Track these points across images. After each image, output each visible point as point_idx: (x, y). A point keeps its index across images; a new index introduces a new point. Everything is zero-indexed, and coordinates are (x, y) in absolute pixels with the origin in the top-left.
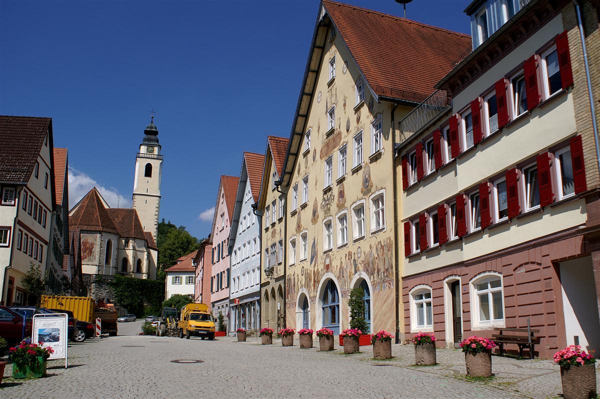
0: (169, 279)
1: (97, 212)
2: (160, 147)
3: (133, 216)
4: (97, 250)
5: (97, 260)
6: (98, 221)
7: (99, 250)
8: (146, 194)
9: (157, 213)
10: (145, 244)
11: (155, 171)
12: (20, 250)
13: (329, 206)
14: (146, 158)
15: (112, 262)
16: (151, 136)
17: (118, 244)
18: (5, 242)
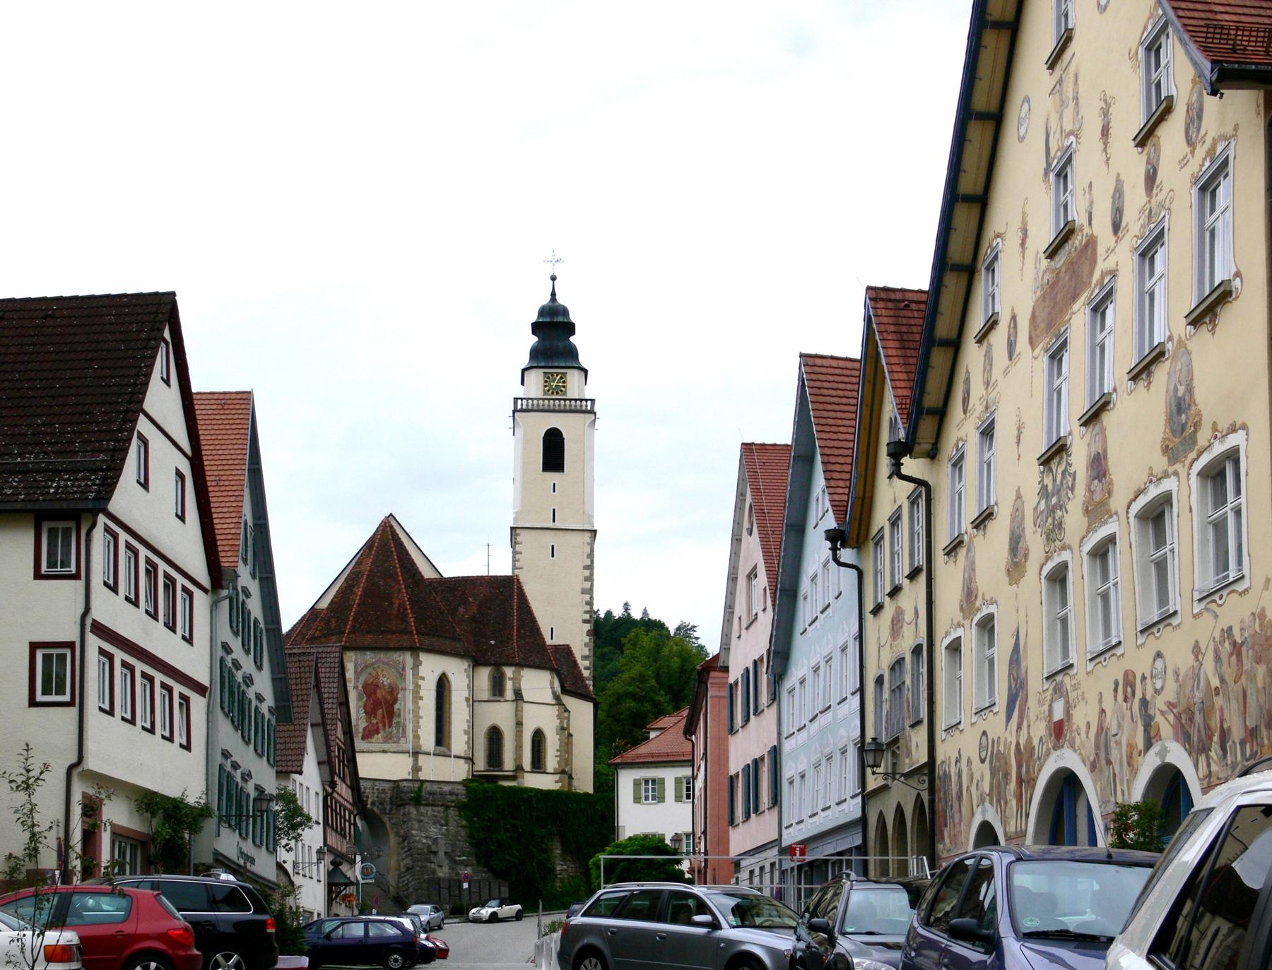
0: (626, 781)
1: (400, 590)
3: (511, 597)
6: (404, 618)
8: (551, 525)
10: (552, 683)
12: (111, 712)
13: (1059, 513)
15: (459, 743)
17: (472, 688)
18: (61, 691)
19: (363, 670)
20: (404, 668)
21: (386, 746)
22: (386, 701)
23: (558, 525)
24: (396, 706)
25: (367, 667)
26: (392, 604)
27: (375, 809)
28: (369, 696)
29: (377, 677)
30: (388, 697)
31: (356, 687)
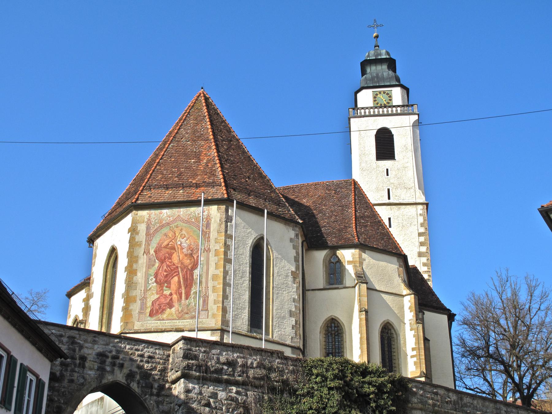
1: (210, 147)
4: (212, 270)
5: (214, 308)
6: (212, 174)
7: (220, 272)
8: (387, 201)
9: (424, 249)
11: (403, 141)
14: (370, 116)
16: (380, 69)
19: (156, 231)
20: (208, 225)
21: (180, 324)
22: (184, 267)
23: (392, 201)
24: (197, 272)
25: (162, 227)
26: (199, 161)
27: (134, 386)
28: (162, 261)
30: (187, 261)
31: (147, 252)
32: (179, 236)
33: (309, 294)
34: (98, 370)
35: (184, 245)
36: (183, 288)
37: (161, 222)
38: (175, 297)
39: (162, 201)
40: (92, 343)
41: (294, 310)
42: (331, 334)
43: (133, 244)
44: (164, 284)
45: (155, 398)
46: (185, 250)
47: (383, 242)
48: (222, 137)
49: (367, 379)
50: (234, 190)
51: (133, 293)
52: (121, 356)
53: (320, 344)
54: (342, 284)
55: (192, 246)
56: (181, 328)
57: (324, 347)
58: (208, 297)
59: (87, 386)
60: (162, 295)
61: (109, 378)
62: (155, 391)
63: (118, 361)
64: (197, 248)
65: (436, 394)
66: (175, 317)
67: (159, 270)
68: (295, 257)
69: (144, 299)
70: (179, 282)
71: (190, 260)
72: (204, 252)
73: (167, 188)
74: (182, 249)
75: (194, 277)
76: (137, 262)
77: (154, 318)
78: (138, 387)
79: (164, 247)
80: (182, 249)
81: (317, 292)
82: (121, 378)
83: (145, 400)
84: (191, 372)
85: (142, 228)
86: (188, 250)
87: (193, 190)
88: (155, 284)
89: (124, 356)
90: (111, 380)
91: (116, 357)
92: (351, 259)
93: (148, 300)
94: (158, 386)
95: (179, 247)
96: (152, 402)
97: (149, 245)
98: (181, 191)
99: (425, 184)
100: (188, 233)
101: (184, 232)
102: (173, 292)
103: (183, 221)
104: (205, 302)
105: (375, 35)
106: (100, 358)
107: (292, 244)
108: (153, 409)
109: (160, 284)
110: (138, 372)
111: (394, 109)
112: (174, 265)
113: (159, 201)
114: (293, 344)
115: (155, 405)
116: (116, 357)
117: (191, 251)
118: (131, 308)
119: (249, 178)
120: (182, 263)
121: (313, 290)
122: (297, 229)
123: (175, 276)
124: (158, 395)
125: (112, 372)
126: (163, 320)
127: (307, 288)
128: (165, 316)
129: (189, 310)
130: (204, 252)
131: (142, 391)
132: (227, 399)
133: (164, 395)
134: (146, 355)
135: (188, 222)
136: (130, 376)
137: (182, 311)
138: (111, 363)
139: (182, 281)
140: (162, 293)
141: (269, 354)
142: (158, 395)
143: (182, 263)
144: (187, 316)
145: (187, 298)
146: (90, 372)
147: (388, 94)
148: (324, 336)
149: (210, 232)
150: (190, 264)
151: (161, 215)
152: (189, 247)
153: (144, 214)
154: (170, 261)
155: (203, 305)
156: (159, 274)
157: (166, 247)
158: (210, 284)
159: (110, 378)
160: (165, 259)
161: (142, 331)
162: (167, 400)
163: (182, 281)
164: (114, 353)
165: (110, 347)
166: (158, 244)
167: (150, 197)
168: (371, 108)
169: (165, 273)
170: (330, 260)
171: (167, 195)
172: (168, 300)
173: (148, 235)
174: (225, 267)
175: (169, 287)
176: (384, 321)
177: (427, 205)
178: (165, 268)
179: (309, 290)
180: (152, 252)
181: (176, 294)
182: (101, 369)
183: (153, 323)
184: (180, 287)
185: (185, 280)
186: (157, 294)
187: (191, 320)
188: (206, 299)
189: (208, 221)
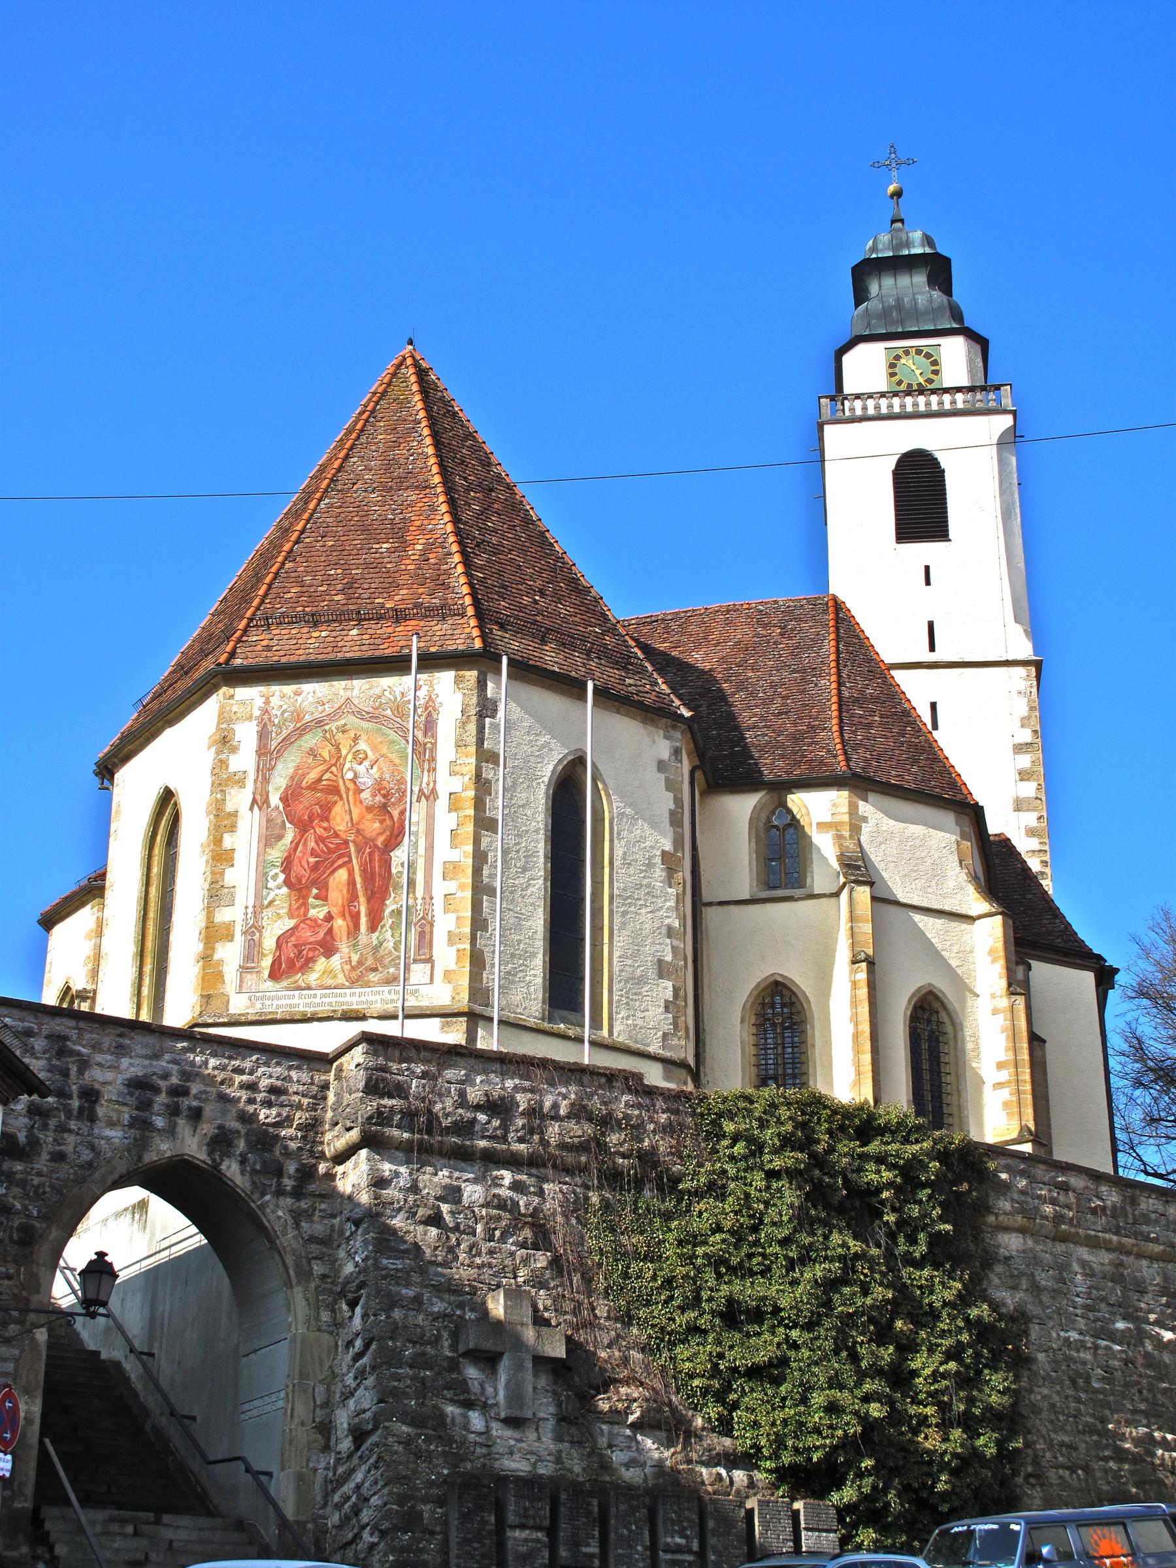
1: (433, 509)
2: (980, 342)
4: (444, 852)
5: (448, 955)
6: (441, 582)
7: (464, 855)
9: (1029, 789)
14: (880, 417)
19: (287, 742)
20: (430, 726)
21: (353, 999)
22: (364, 842)
23: (942, 653)
24: (399, 856)
25: (302, 731)
26: (403, 545)
27: (231, 1169)
28: (303, 827)
29: (337, 760)
30: (373, 827)
31: (259, 801)
32: (350, 757)
33: (711, 915)
34: (131, 1126)
35: (366, 781)
36: (362, 899)
37: (299, 719)
38: (339, 923)
39: (302, 658)
40: (112, 1053)
41: (669, 958)
42: (774, 1025)
43: (223, 780)
44: (309, 888)
45: (289, 1201)
46: (365, 795)
47: (915, 769)
48: (465, 479)
49: (874, 1147)
50: (502, 627)
51: (223, 915)
52: (195, 1089)
53: (743, 1053)
54: (803, 886)
55: (385, 783)
56: (357, 1011)
57: (753, 1060)
58: (432, 926)
59: (103, 1170)
60: (305, 919)
61: (162, 1149)
62: (289, 1184)
63: (185, 1102)
64: (399, 790)
65: (1064, 1187)
66: (341, 979)
67: (295, 850)
68: (672, 813)
69: (253, 930)
70: (351, 882)
71: (382, 822)
72: (419, 800)
73: (315, 621)
74: (359, 791)
75: (394, 871)
76: (232, 828)
77: (284, 984)
78: (243, 1173)
79: (308, 788)
80: (359, 791)
81: (732, 907)
82: (194, 1147)
83: (263, 1207)
84: (387, 1131)
85: (246, 735)
86: (374, 796)
87: (386, 628)
88: (285, 890)
89: (203, 1088)
90: (168, 1154)
91: (179, 1092)
92: (829, 819)
93: (266, 933)
94: (297, 1170)
95: (351, 786)
96: (280, 1213)
97: (266, 781)
98: (355, 632)
99: (1035, 606)
100: (374, 748)
101: (362, 745)
102: (334, 911)
103: (360, 714)
104: (425, 939)
105: (891, 188)
106: (137, 1093)
107: (662, 776)
108: (285, 1234)
109: (300, 890)
110: (243, 1132)
111: (947, 398)
112: (336, 835)
113: (293, 659)
114: (667, 1054)
115: (290, 1221)
116: (179, 1092)
117: (384, 796)
118: (216, 957)
119: (542, 593)
120: (358, 832)
121: (721, 903)
122: (678, 735)
123: (340, 867)
124: (297, 1194)
125: (171, 1131)
126: (309, 988)
127: (706, 896)
128: (312, 978)
129: (379, 960)
130: (419, 800)
131: (254, 1183)
132: (486, 1205)
133: (312, 1195)
134: (264, 1083)
135: (373, 717)
136: (221, 1142)
137: (360, 963)
138: (168, 1106)
139: (358, 879)
140: (307, 911)
141: (603, 1080)
142: (297, 1194)
143: (358, 832)
144: (373, 977)
145: (373, 928)
146: (109, 1133)
147: (928, 356)
148: (753, 1030)
149: (434, 744)
150: (380, 834)
151: (300, 699)
152: (379, 787)
153: (250, 695)
154: (325, 825)
155: (419, 947)
156: (296, 862)
157: (313, 786)
158: (440, 887)
159: (164, 1147)
160: (311, 820)
161: (250, 1018)
162: (323, 1206)
163: (358, 879)
164: (175, 1080)
165: (163, 1064)
166: (292, 778)
167: (268, 648)
168: (883, 395)
169: (312, 860)
170: (769, 820)
171: (313, 643)
172: (321, 934)
173: (265, 754)
174: (477, 841)
175: (323, 897)
176: (919, 989)
177: (1038, 665)
178: (312, 844)
179: (710, 904)
180: (275, 800)
181: (344, 917)
182: (141, 1124)
183: (280, 998)
184: (353, 897)
185: (368, 877)
186: (291, 916)
187: (386, 989)
188: (427, 929)
189: (429, 714)
